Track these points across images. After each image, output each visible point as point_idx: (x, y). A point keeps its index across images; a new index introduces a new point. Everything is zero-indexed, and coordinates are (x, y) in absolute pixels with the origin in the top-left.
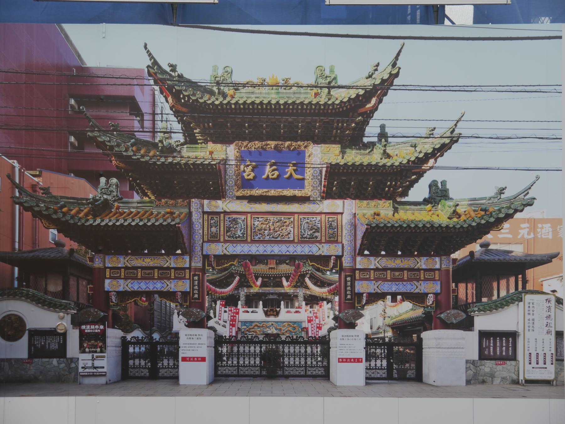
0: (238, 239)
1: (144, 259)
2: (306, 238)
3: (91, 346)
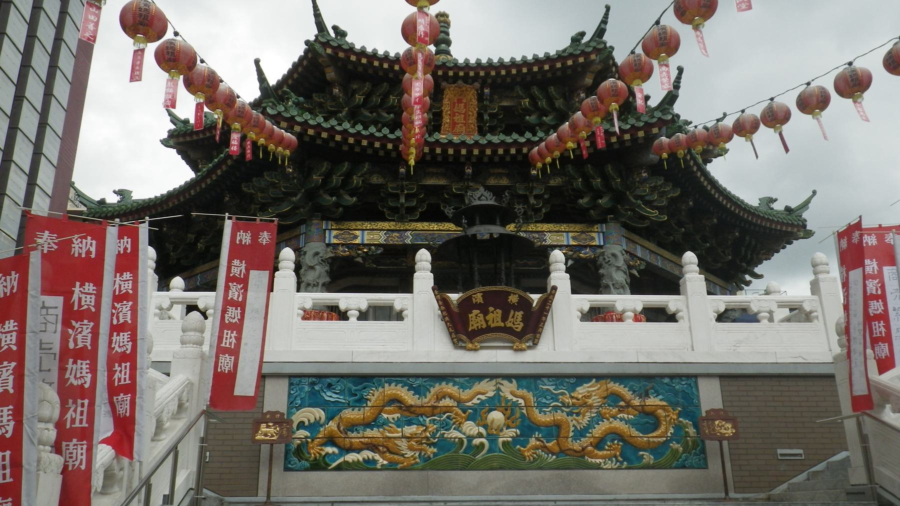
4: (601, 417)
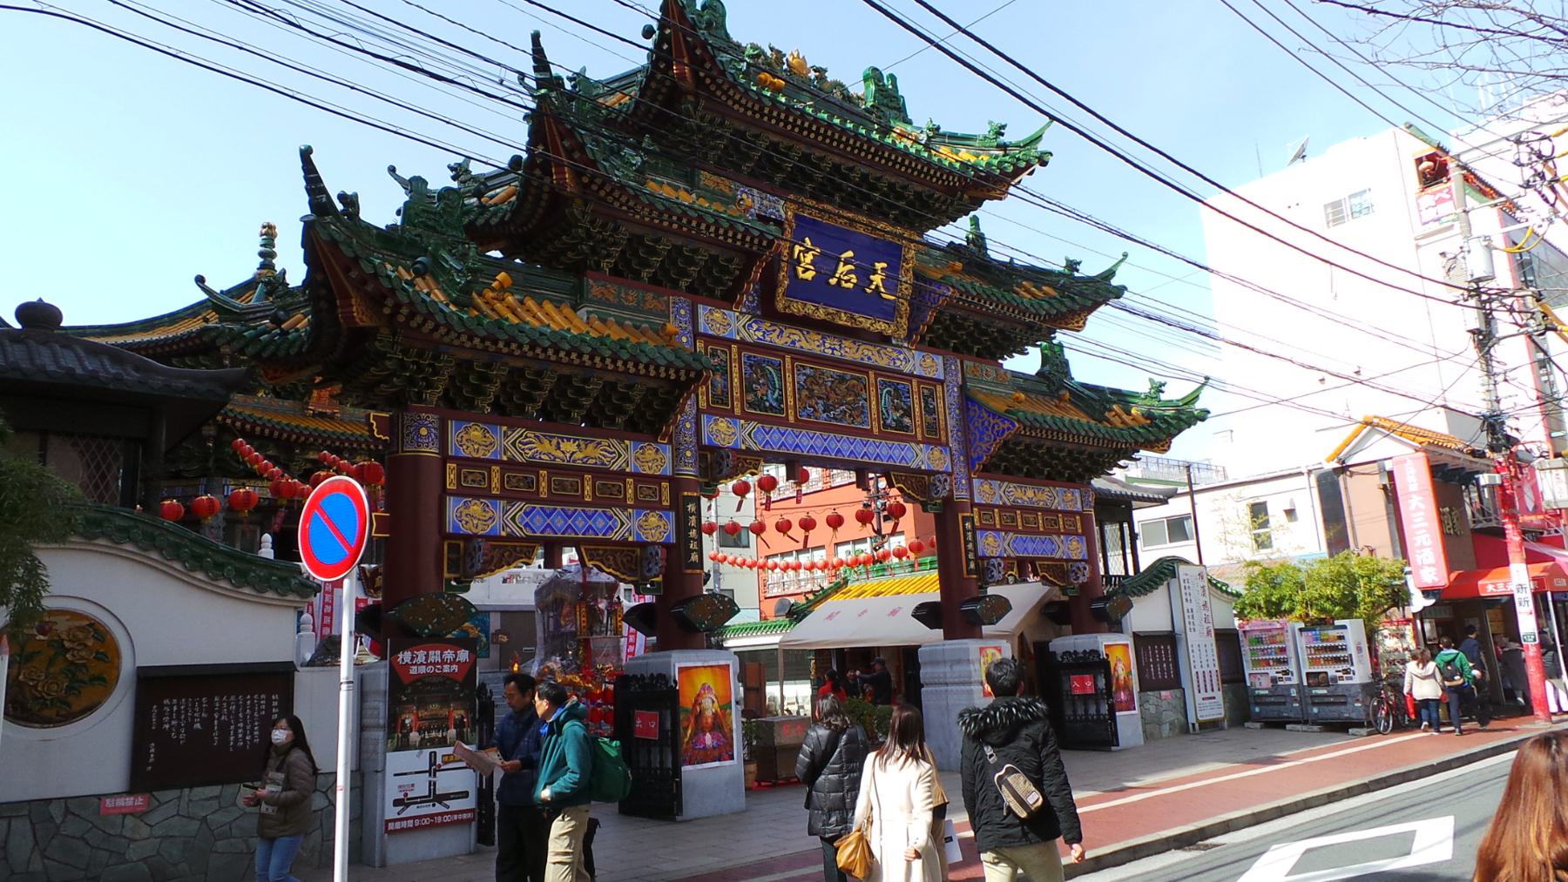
1: (558, 443)
3: (426, 723)
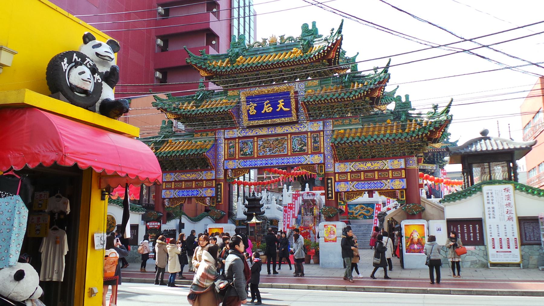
0: (248, 156)
2: (297, 151)
4: (360, 211)
